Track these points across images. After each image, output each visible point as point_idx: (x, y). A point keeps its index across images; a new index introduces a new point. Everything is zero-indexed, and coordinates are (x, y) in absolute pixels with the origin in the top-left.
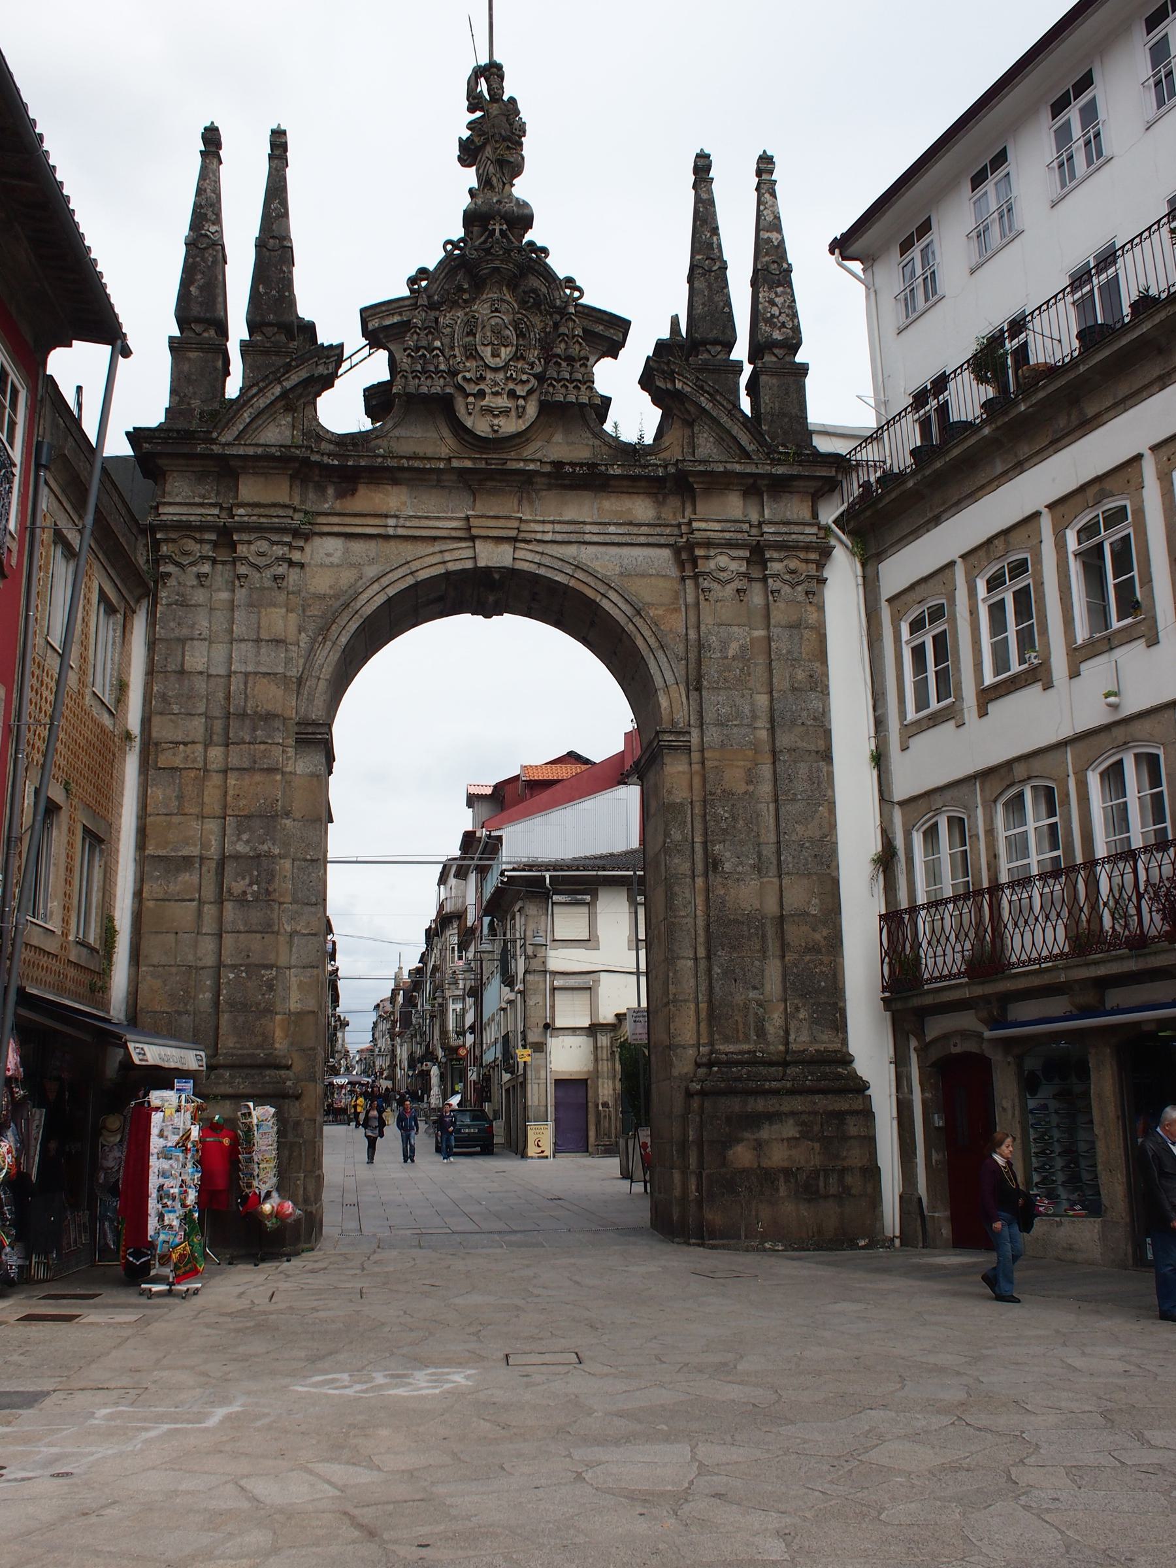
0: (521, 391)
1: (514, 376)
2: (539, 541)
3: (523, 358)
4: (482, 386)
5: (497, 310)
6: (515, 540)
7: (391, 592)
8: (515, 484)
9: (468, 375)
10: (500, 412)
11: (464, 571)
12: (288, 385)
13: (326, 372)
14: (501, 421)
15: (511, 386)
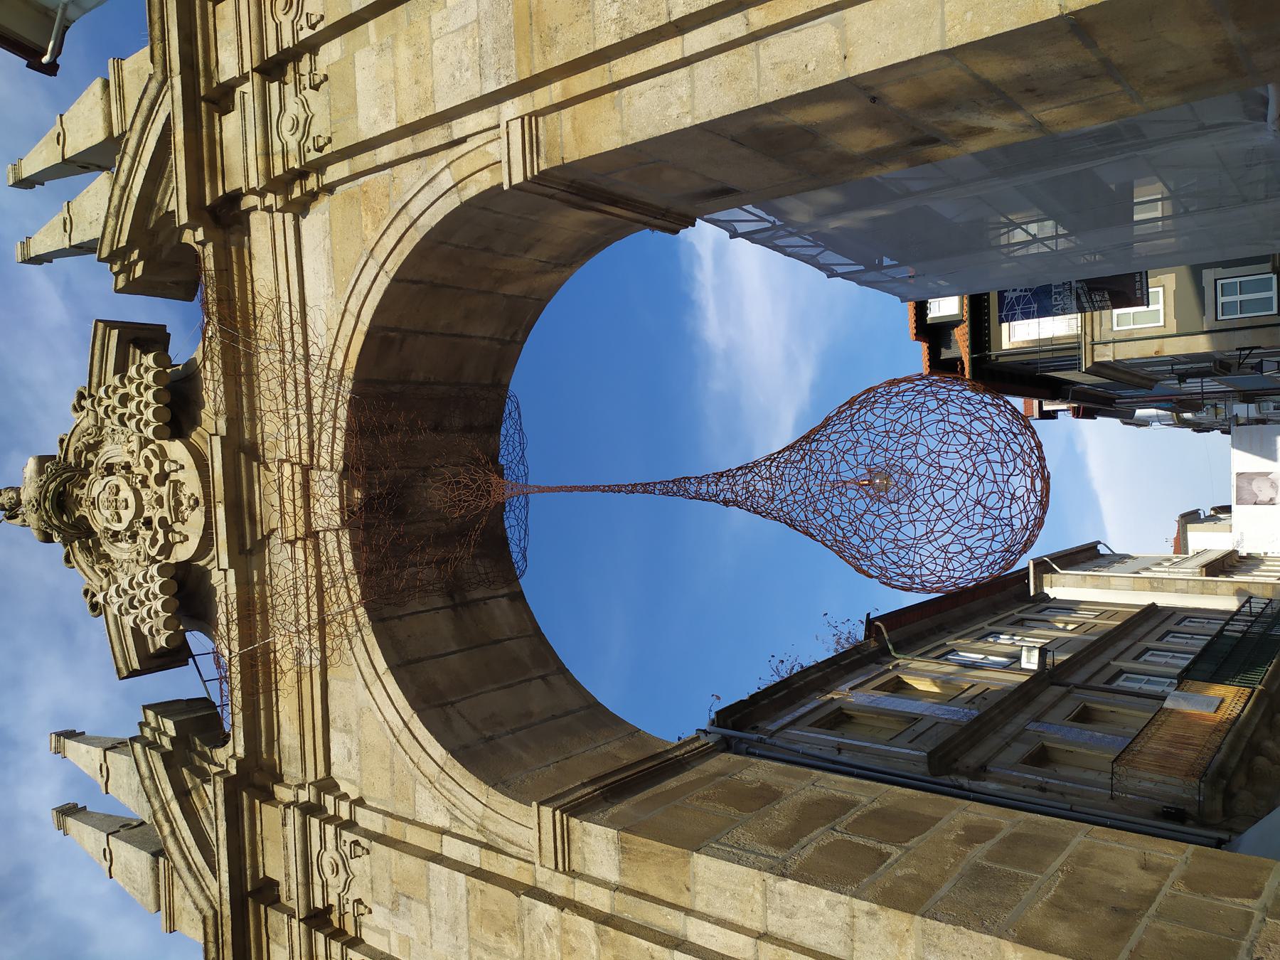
0: (156, 469)
1: (140, 478)
2: (310, 433)
3: (127, 467)
4: (156, 523)
5: (93, 503)
6: (306, 470)
7: (381, 665)
8: (255, 470)
9: (148, 543)
10: (175, 494)
11: (355, 548)
12: (169, 793)
13: (173, 733)
14: (187, 490)
15: (151, 482)
